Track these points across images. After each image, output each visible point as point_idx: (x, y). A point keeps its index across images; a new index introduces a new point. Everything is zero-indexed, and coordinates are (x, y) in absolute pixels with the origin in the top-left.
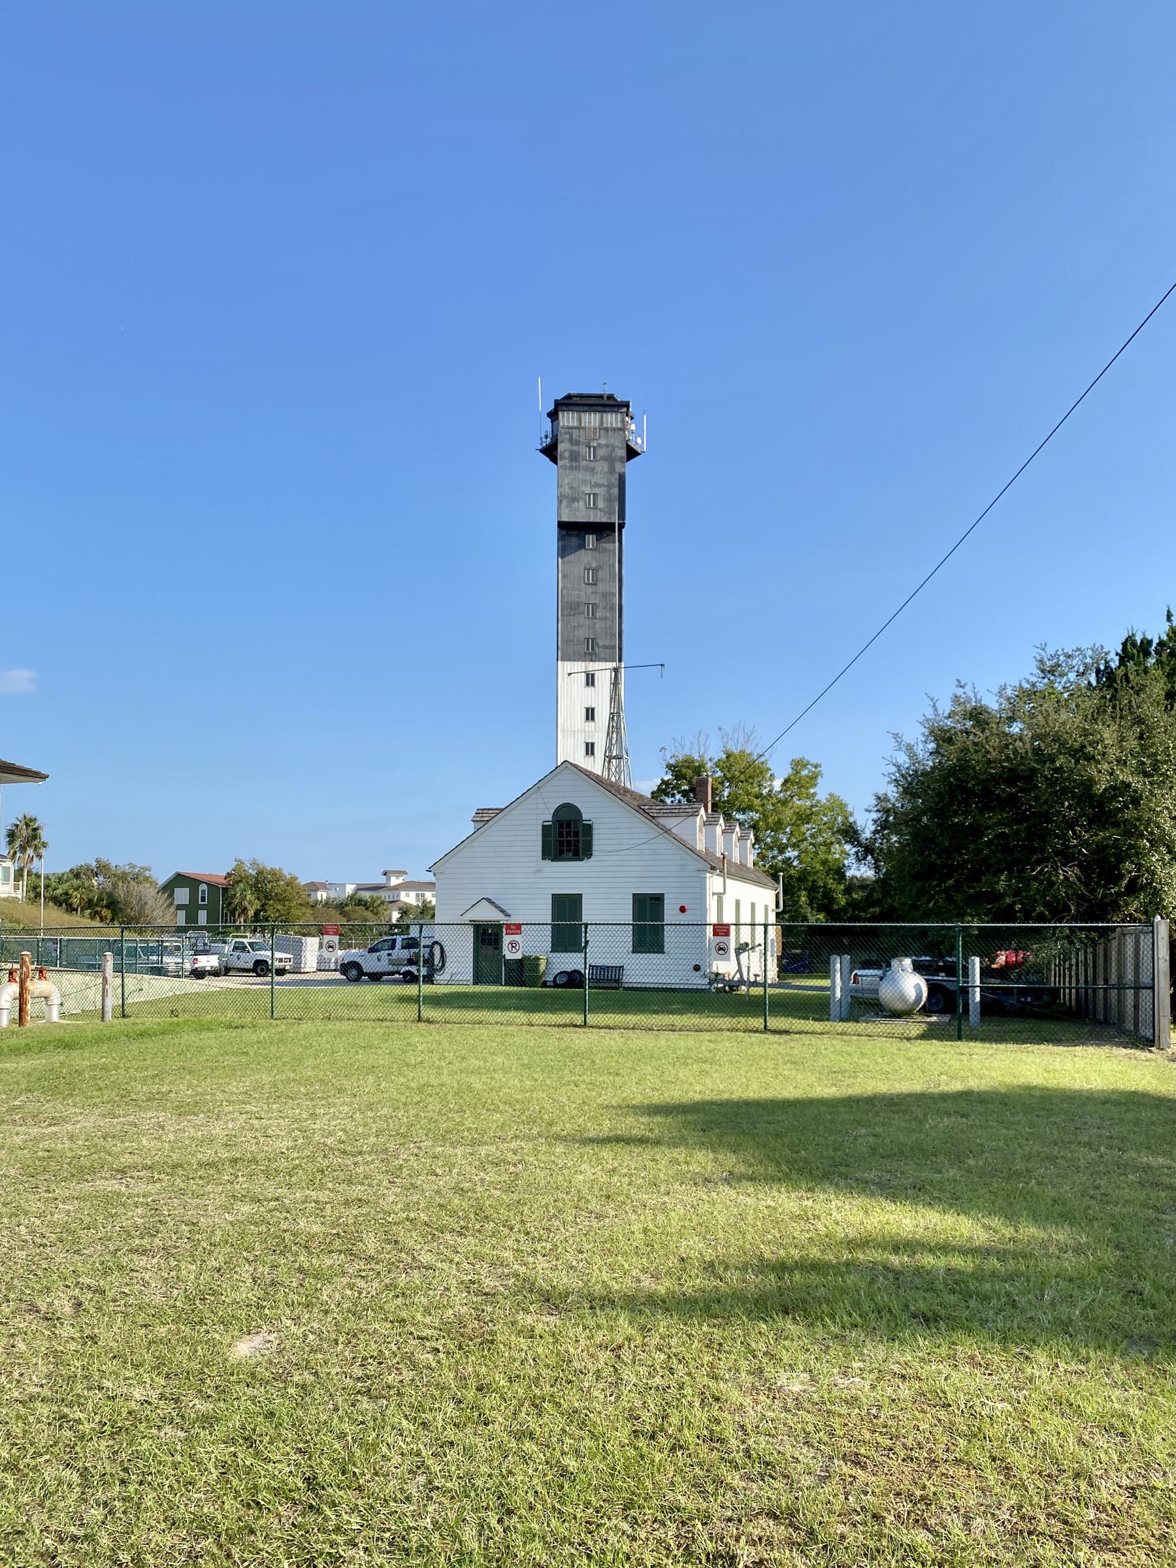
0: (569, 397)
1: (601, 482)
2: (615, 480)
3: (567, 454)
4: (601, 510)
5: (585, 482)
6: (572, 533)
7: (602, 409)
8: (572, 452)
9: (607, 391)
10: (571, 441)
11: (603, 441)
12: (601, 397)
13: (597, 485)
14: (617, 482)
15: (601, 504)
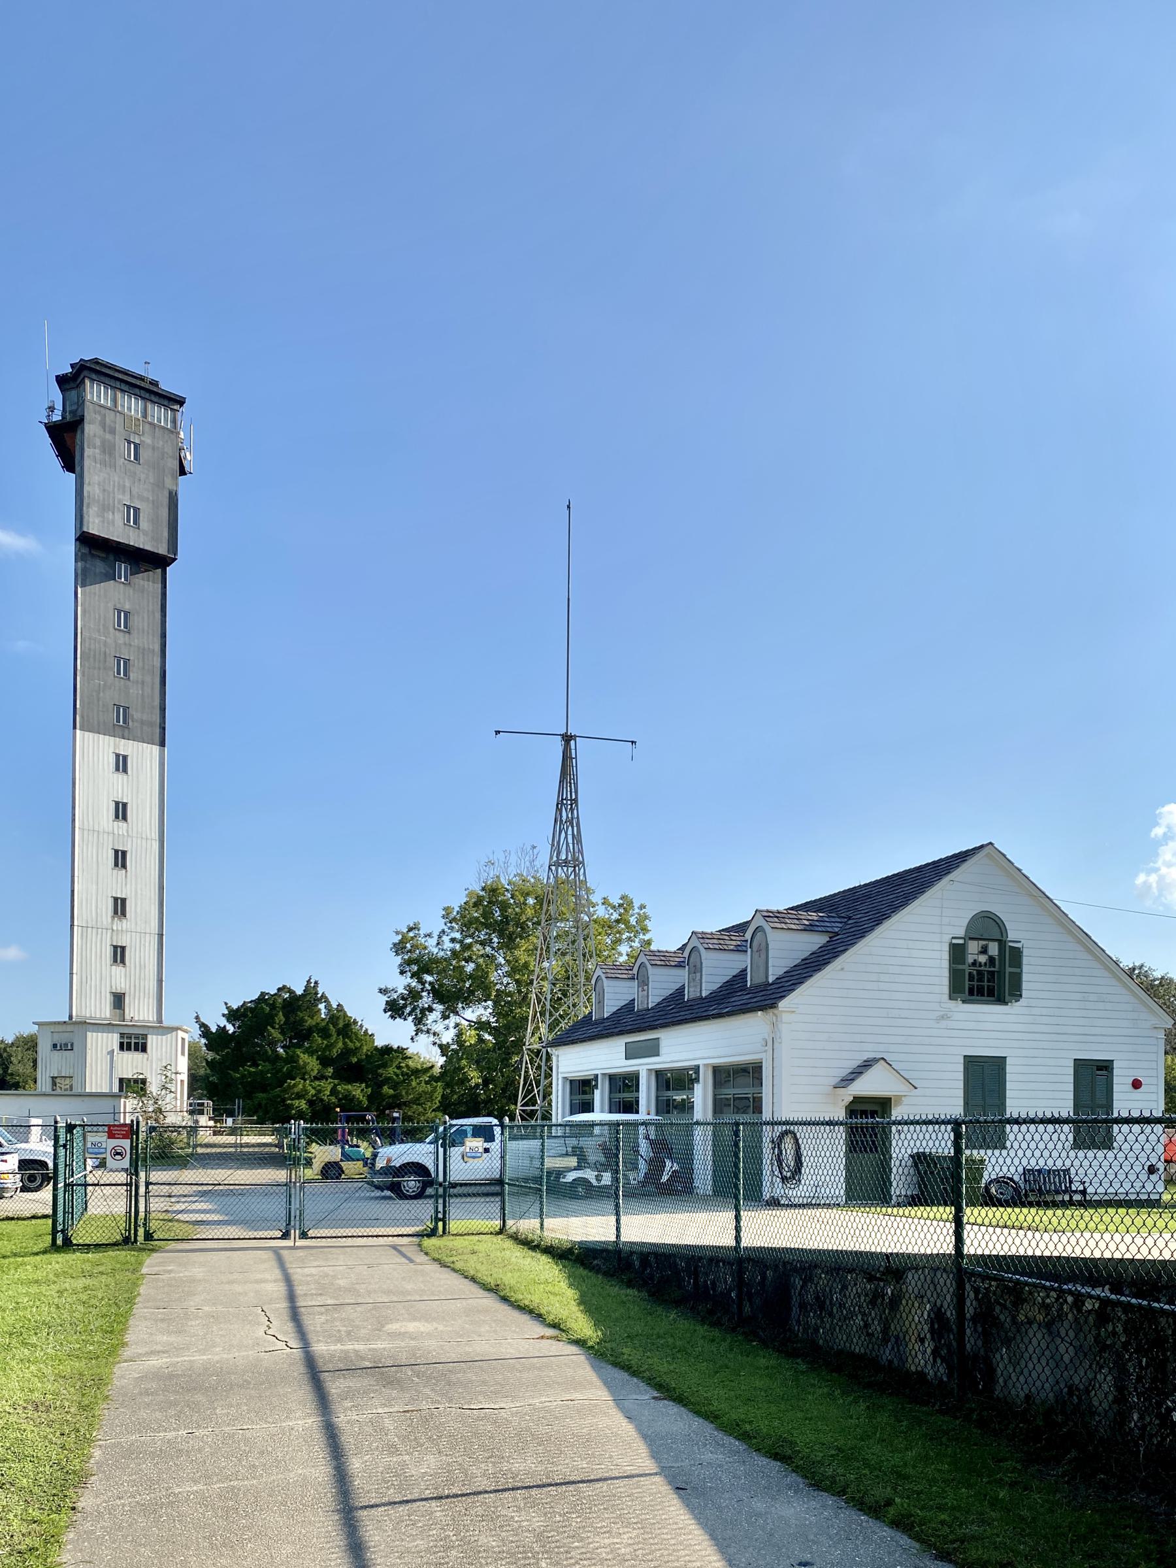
0: (96, 361)
1: (145, 494)
2: (165, 501)
3: (98, 442)
4: (145, 533)
5: (123, 489)
6: (100, 554)
7: (143, 393)
8: (103, 442)
9: (152, 375)
10: (103, 424)
11: (148, 440)
12: (142, 379)
13: (141, 498)
14: (166, 501)
15: (144, 524)
